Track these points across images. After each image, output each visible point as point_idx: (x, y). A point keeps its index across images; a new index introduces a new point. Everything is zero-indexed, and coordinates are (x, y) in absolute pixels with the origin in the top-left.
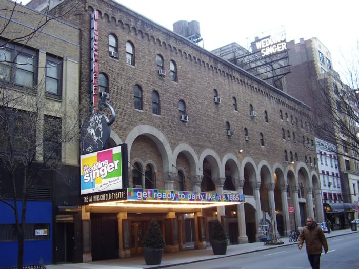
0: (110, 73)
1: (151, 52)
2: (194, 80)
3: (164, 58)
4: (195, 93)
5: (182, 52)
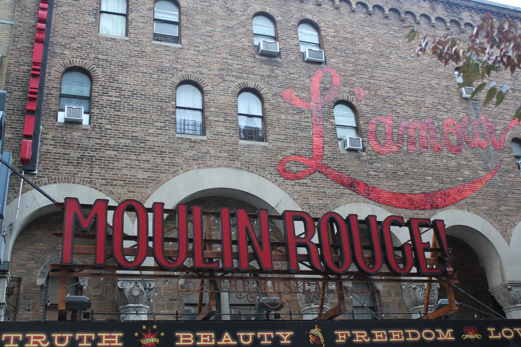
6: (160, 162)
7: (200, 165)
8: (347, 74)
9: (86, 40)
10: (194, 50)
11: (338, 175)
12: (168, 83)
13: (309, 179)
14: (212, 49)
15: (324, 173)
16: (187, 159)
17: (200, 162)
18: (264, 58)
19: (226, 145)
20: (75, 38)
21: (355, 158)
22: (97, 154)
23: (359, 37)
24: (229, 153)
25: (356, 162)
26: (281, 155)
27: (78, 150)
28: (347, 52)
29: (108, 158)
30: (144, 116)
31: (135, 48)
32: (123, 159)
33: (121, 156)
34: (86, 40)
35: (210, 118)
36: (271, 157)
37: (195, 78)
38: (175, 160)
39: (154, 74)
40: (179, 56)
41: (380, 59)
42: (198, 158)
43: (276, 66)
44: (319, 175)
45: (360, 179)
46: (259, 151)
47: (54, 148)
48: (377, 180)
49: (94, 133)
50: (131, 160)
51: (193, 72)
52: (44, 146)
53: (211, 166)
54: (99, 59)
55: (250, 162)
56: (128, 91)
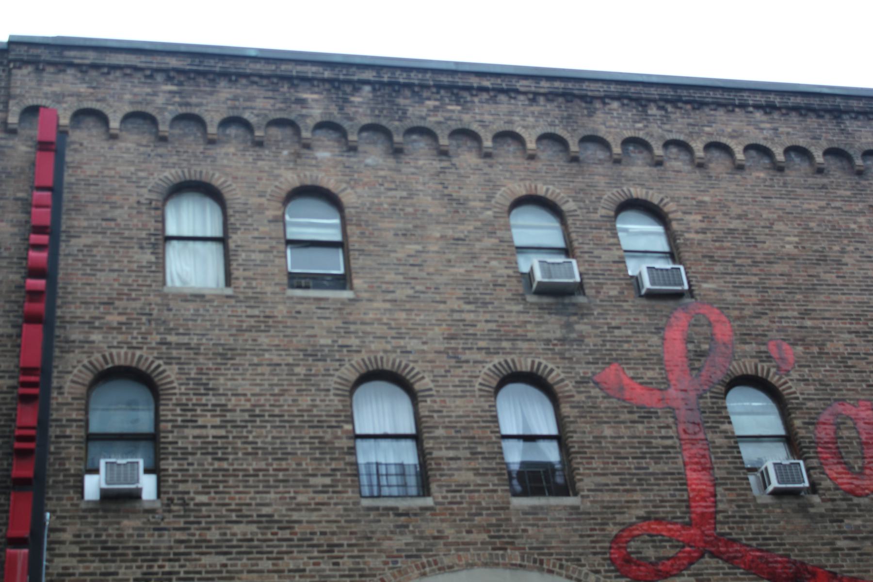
0: (169, 360)
1: (461, 203)
2: (823, 259)
3: (568, 206)
4: (857, 319)
5: (698, 146)
6: (331, 570)
7: (424, 567)
8: (747, 312)
9: (138, 305)
10: (384, 301)
11: (758, 557)
12: (332, 382)
13: (689, 575)
14: (423, 292)
15: (725, 556)
16: (393, 557)
17: (424, 560)
18: (546, 300)
19: (480, 514)
20: (112, 303)
21: (795, 511)
22: (182, 566)
23: (762, 223)
24: (489, 531)
25: (800, 521)
26: (615, 524)
27: (135, 561)
28: (738, 261)
29: (207, 572)
30: (284, 464)
31: (250, 312)
32: (241, 572)
33: (236, 565)
34: (138, 305)
35: (436, 454)
36: (592, 530)
37: (393, 364)
38: (365, 563)
39: (298, 365)
40: (351, 318)
41: (819, 270)
42: (418, 550)
43: (575, 314)
44: (713, 562)
45: (815, 563)
46: (560, 519)
47: (79, 562)
48: (859, 560)
49: (169, 518)
50: (261, 572)
51: (385, 351)
52: (56, 560)
53: (450, 567)
54: (170, 344)
55: (542, 548)
56: (243, 411)
